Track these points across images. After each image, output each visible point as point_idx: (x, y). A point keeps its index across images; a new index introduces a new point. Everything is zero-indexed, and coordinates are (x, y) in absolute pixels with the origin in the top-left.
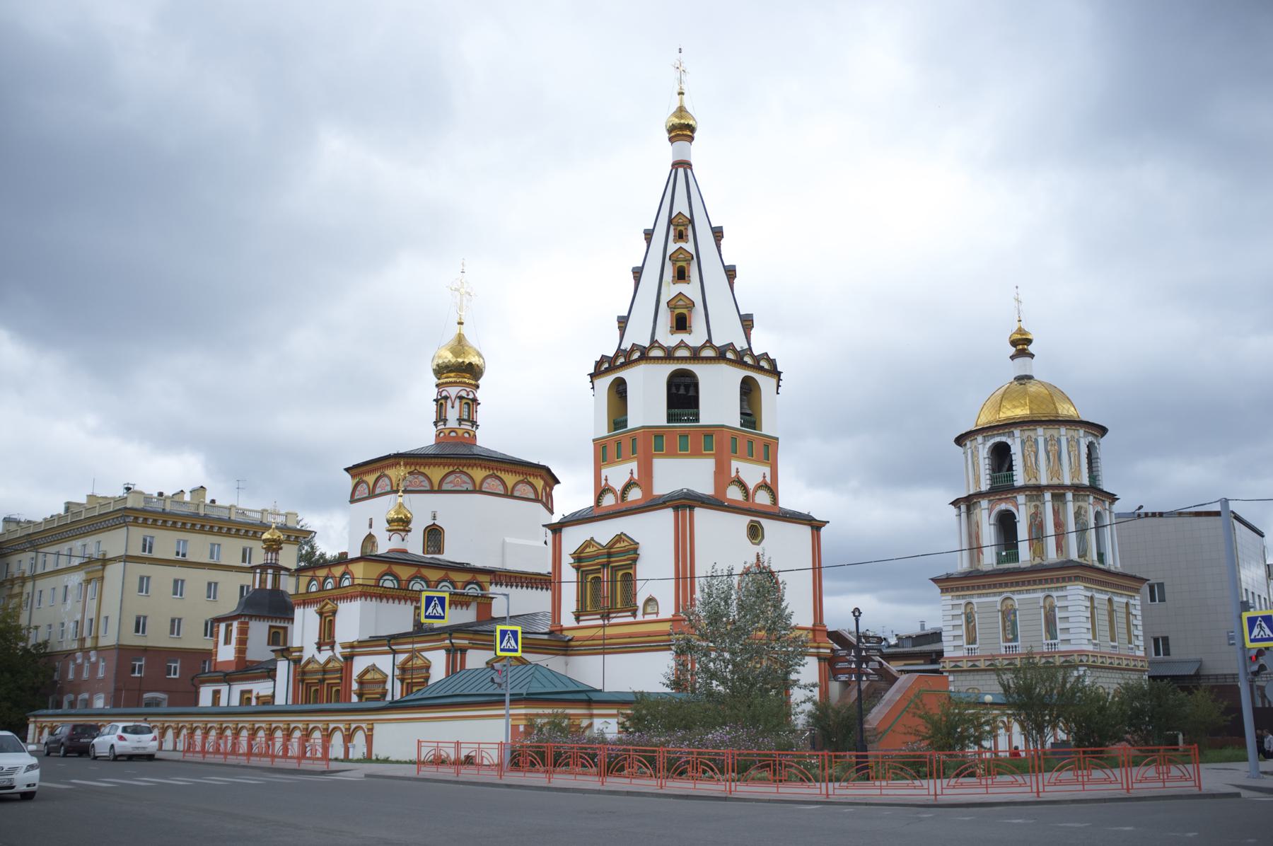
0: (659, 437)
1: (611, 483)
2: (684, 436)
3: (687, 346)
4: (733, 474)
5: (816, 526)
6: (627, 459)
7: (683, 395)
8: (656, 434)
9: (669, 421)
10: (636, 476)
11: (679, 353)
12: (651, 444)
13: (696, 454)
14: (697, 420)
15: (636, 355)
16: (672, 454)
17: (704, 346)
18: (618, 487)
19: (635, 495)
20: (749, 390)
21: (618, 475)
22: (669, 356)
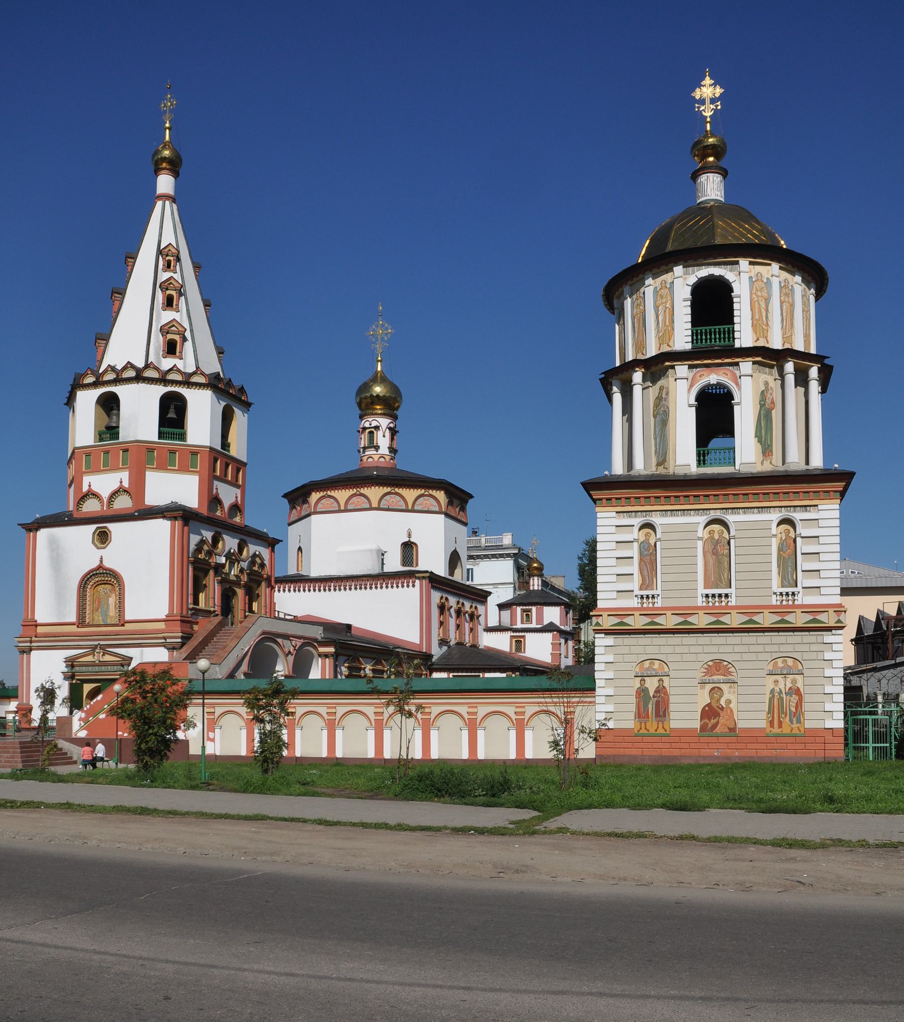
0: (151, 450)
1: (95, 488)
2: (173, 452)
3: (179, 371)
4: (215, 491)
5: (272, 543)
6: (116, 469)
7: (172, 414)
8: (148, 448)
9: (160, 438)
10: (126, 484)
11: (171, 377)
12: (142, 458)
13: (184, 469)
14: (182, 437)
15: (131, 373)
16: (162, 467)
17: (194, 373)
18: (105, 495)
19: (124, 503)
20: (227, 418)
21: (104, 483)
22: (163, 380)
